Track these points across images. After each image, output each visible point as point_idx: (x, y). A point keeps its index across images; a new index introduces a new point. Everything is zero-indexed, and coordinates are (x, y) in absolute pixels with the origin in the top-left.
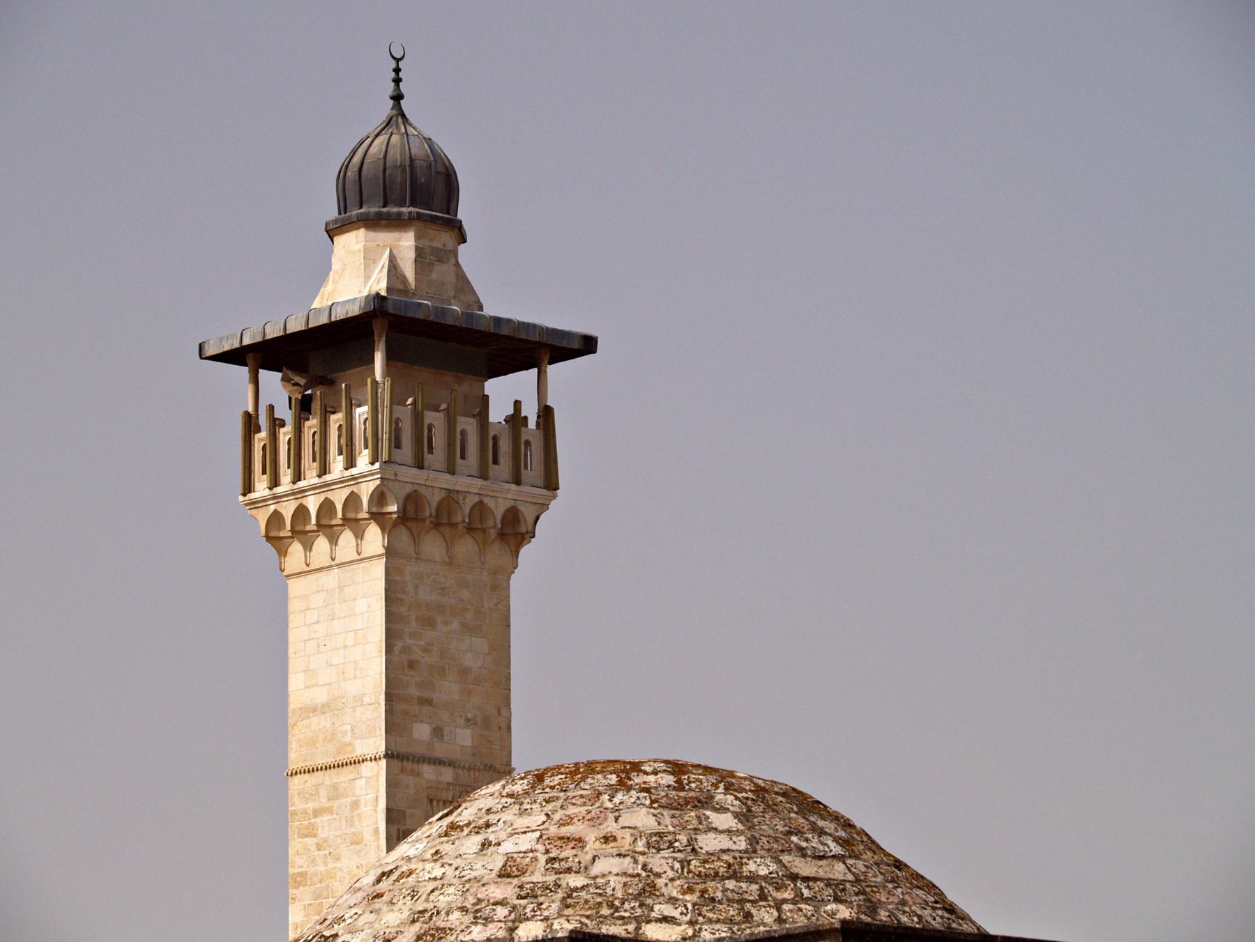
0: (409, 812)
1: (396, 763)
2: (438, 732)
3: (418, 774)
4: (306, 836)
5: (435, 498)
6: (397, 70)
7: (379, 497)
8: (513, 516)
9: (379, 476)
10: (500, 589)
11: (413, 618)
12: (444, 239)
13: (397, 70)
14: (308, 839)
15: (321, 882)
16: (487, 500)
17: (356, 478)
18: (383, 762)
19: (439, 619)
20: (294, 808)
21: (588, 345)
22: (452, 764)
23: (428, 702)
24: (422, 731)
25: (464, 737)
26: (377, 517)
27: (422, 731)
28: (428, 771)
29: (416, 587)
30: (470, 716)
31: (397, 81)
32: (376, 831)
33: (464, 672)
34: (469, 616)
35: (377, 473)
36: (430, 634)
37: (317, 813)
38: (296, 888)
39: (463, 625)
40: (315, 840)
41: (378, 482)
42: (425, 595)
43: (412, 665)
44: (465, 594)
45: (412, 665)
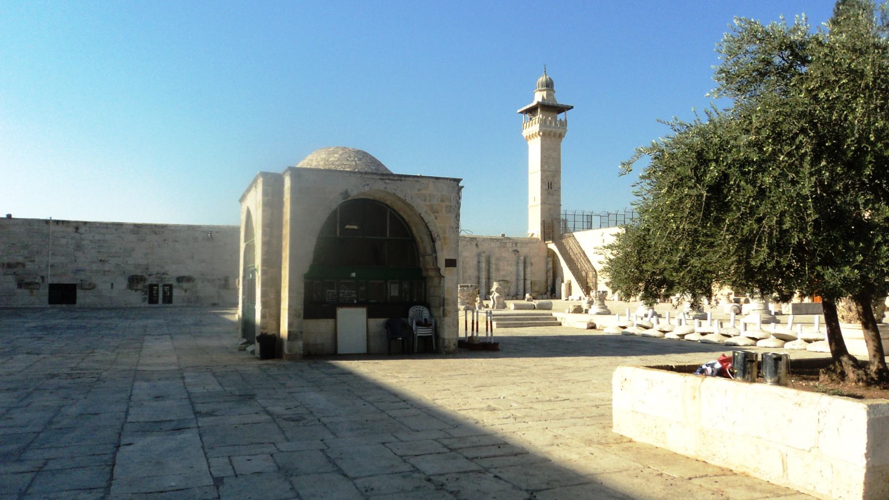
2: (549, 167)
7: (539, 132)
10: (559, 145)
12: (552, 92)
21: (572, 107)
25: (553, 167)
26: (539, 135)
27: (546, 167)
28: (547, 172)
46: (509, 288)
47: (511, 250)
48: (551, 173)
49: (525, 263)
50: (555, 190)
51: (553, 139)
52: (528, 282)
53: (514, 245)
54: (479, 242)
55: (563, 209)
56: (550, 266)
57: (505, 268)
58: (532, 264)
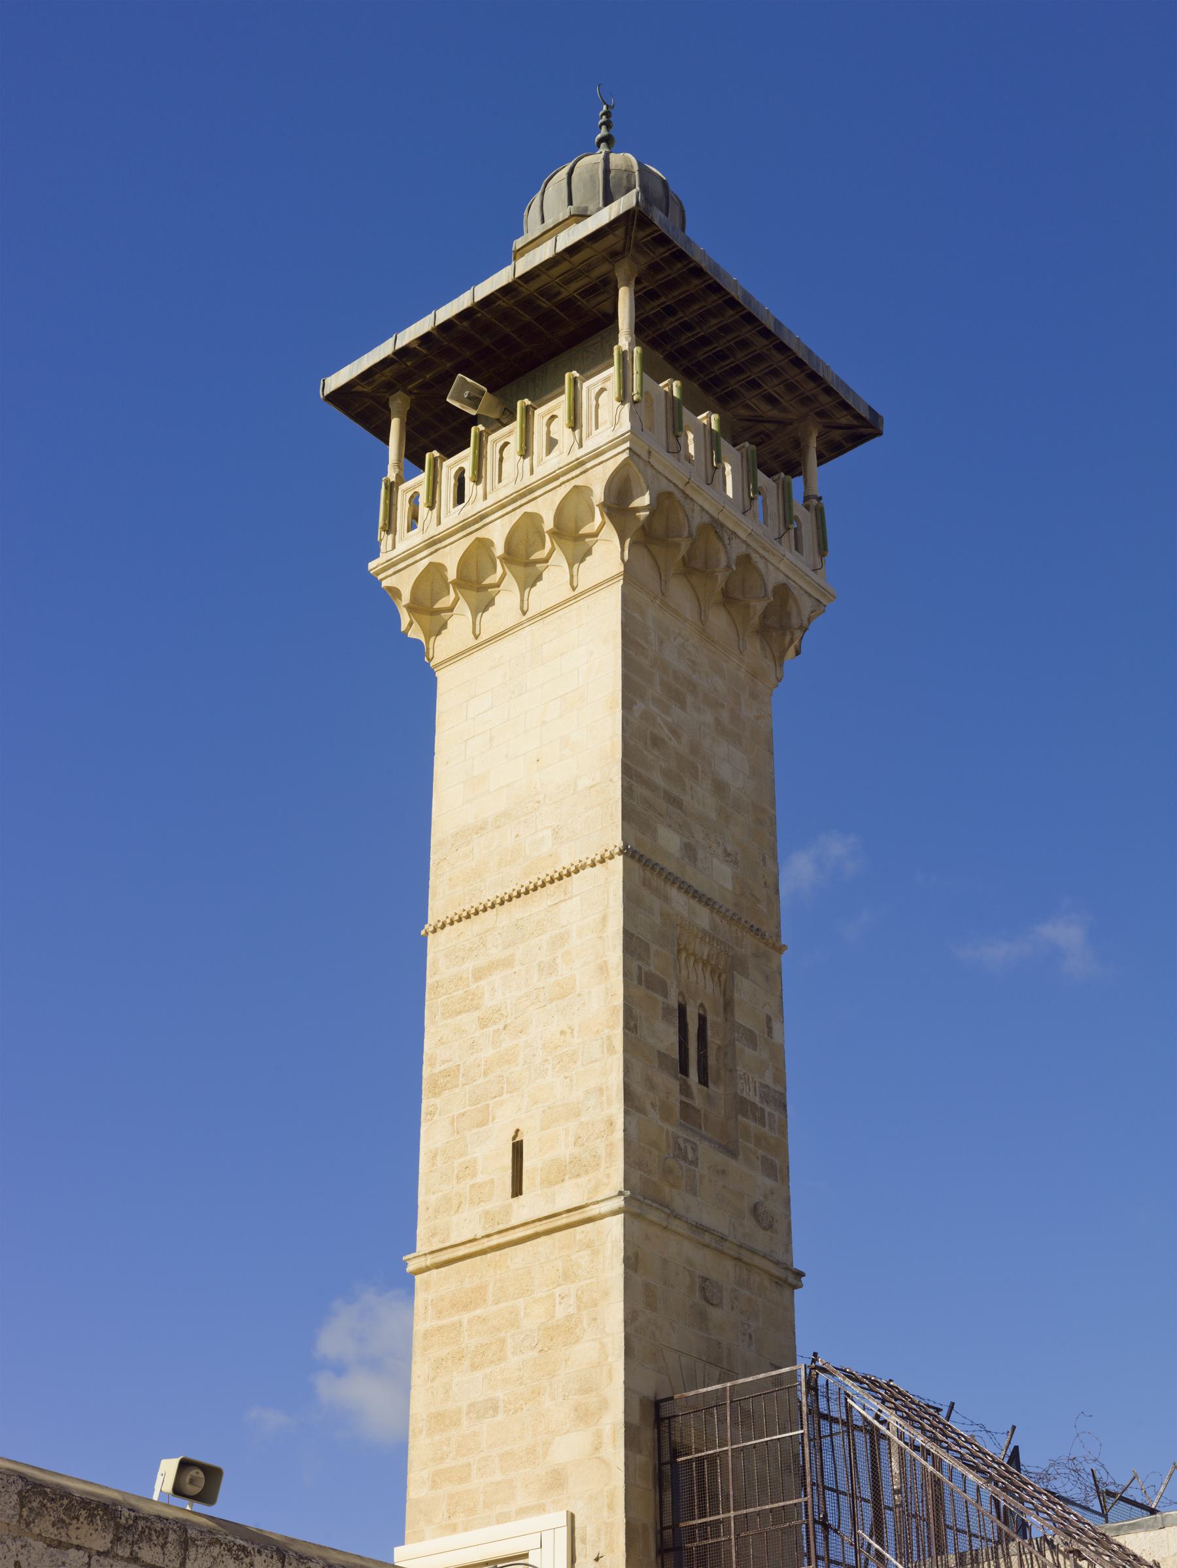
0: (654, 948)
1: (635, 865)
2: (689, 850)
4: (459, 1013)
5: (697, 519)
9: (627, 445)
14: (463, 1016)
15: (485, 1074)
16: (754, 556)
17: (582, 463)
18: (619, 860)
19: (689, 699)
20: (437, 978)
22: (707, 902)
23: (677, 803)
30: (729, 849)
32: (603, 969)
33: (720, 788)
35: (624, 442)
37: (478, 975)
38: (435, 1095)
39: (718, 721)
40: (476, 1014)
41: (626, 455)
45: (656, 742)
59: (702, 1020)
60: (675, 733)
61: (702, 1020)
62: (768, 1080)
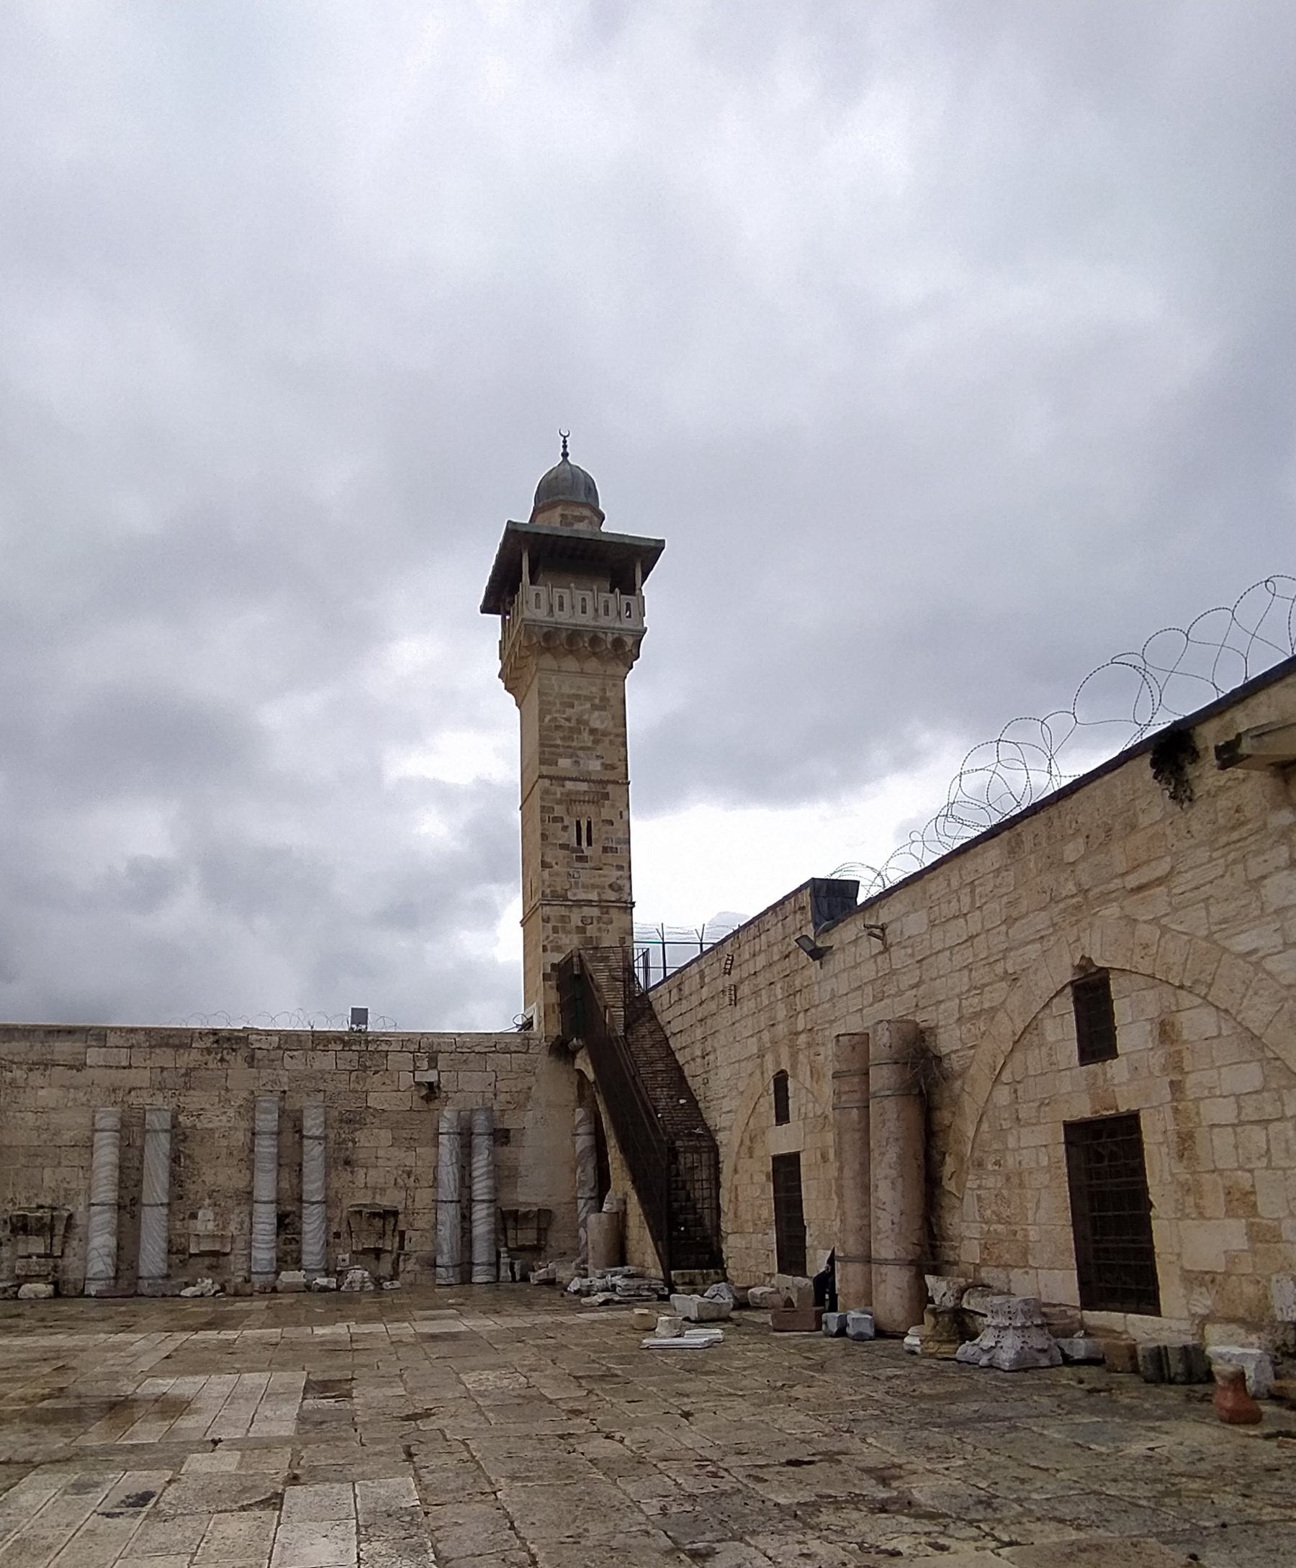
3: (563, 786)
6: (565, 442)
8: (618, 643)
11: (558, 702)
13: (565, 442)
19: (576, 703)
24: (564, 763)
29: (560, 687)
31: (565, 447)
33: (593, 731)
34: (597, 701)
36: (569, 712)
42: (566, 690)
43: (558, 727)
44: (594, 689)
45: (558, 727)
46: (402, 1234)
47: (406, 1079)
48: (583, 787)
49: (465, 1136)
50: (605, 850)
51: (592, 665)
52: (481, 1213)
53: (425, 1065)
54: (259, 1054)
55: (644, 919)
56: (583, 1142)
57: (381, 1153)
58: (501, 1137)
59: (589, 823)
60: (568, 720)
61: (589, 823)
62: (620, 835)
